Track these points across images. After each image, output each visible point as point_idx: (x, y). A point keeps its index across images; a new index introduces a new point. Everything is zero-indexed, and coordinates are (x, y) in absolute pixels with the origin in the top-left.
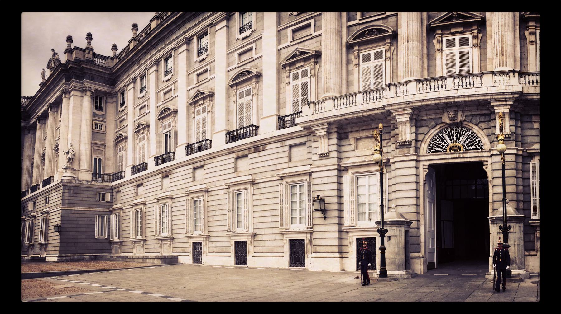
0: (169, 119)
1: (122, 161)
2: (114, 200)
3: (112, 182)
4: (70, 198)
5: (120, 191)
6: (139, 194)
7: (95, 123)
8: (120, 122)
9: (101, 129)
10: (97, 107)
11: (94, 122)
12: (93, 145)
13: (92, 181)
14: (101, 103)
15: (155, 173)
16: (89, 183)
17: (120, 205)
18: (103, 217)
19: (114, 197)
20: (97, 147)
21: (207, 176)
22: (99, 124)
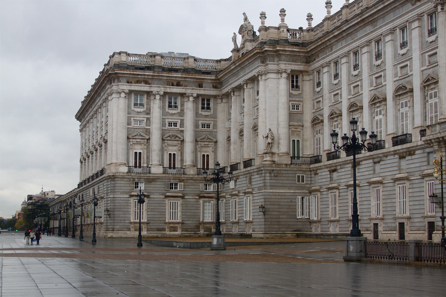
1: (320, 144)
3: (311, 164)
4: (271, 181)
5: (318, 174)
6: (334, 179)
7: (292, 104)
8: (317, 102)
9: (298, 109)
10: (293, 87)
11: (290, 103)
12: (291, 127)
13: (291, 164)
14: (297, 82)
16: (288, 166)
20: (295, 128)
22: (296, 104)
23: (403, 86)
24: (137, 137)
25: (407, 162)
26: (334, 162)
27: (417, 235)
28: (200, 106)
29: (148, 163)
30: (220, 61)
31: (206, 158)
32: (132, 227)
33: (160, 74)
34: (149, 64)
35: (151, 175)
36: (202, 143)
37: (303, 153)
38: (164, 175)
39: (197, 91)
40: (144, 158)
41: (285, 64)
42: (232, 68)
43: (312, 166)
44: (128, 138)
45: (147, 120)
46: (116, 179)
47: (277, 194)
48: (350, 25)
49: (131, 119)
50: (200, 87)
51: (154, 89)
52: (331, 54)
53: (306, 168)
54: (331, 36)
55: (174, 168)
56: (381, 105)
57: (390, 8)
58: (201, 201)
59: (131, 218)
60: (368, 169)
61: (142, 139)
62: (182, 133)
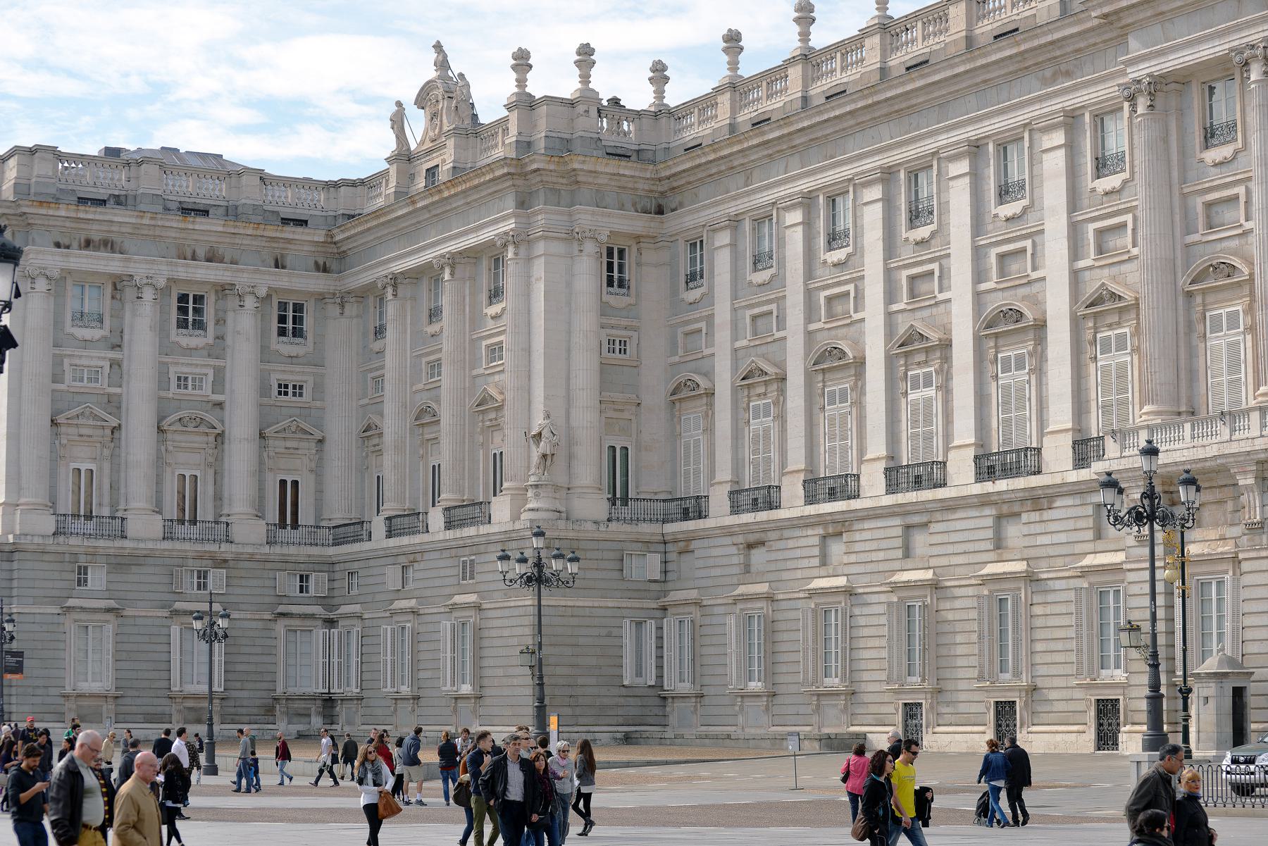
0: (842, 378)
1: (697, 462)
2: (670, 576)
3: (664, 522)
6: (753, 569)
8: (686, 334)
10: (610, 283)
11: (604, 332)
13: (609, 520)
15: (802, 522)
16: (602, 528)
17: (693, 594)
18: (639, 624)
19: (670, 567)
20: (615, 410)
21: (936, 550)
22: (617, 336)
23: (1011, 309)
24: (81, 421)
25: (1025, 530)
26: (758, 519)
27: (1059, 737)
28: (275, 325)
29: (114, 505)
30: (335, 185)
31: (289, 493)
32: (70, 710)
33: (160, 223)
34: (120, 187)
35: (126, 543)
36: (277, 443)
37: (637, 487)
38: (167, 545)
39: (267, 277)
40: (100, 488)
41: (593, 213)
42: (400, 213)
43: (670, 528)
44: (54, 423)
45: (111, 366)
46: (17, 556)
47: (569, 612)
48: (826, 117)
49: (62, 364)
50: (277, 266)
51: (139, 268)
52: (748, 194)
53: (653, 534)
54: (755, 142)
55: (194, 521)
56: (933, 360)
57: (970, 82)
58: (280, 627)
59: (67, 681)
60: (884, 544)
61: (95, 427)
62: (217, 410)
